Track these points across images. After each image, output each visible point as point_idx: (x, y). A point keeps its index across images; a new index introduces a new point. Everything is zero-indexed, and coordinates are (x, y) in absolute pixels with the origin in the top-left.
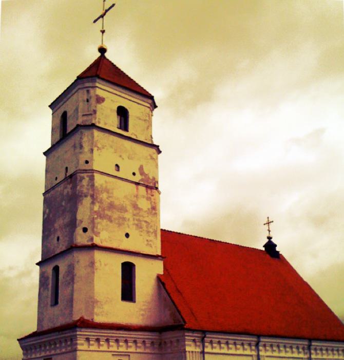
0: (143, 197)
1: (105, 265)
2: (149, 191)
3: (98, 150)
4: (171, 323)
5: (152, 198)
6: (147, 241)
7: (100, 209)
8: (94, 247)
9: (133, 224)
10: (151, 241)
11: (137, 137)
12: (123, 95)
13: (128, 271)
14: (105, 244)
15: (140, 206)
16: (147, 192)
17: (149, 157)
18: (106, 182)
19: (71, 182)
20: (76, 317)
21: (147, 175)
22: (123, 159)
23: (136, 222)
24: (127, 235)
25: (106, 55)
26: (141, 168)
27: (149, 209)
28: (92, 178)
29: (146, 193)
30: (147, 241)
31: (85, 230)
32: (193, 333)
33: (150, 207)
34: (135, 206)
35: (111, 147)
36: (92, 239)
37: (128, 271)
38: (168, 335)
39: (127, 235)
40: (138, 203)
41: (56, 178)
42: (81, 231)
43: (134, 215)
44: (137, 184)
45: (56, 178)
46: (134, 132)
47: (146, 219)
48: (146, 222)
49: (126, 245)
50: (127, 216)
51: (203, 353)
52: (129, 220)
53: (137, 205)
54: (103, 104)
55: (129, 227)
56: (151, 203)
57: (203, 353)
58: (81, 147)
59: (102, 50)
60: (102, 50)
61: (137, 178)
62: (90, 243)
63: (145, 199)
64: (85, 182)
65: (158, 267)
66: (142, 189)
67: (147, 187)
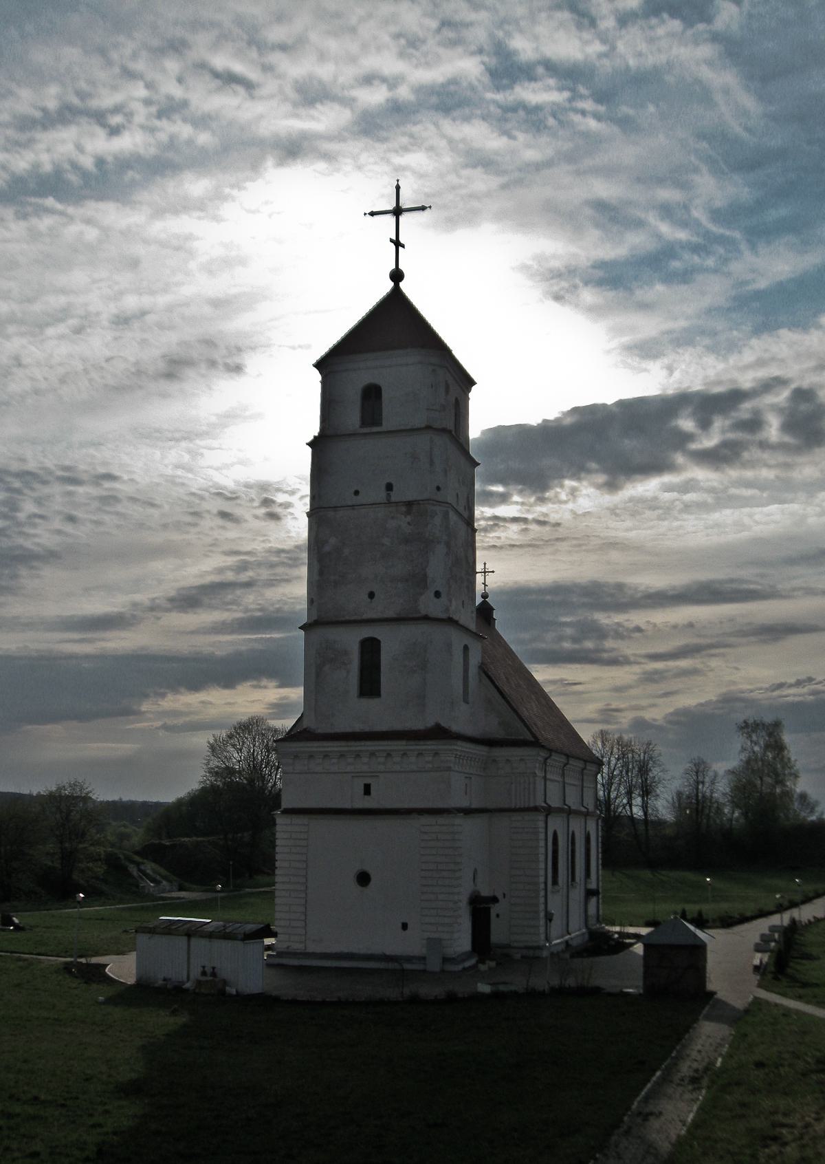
4: (500, 734)
8: (451, 621)
19: (408, 513)
20: (430, 722)
25: (402, 285)
28: (446, 515)
31: (437, 594)
36: (447, 610)
38: (501, 753)
41: (357, 493)
42: (432, 595)
45: (357, 493)
57: (545, 778)
58: (432, 463)
59: (397, 276)
60: (397, 276)
62: (444, 616)
64: (438, 520)
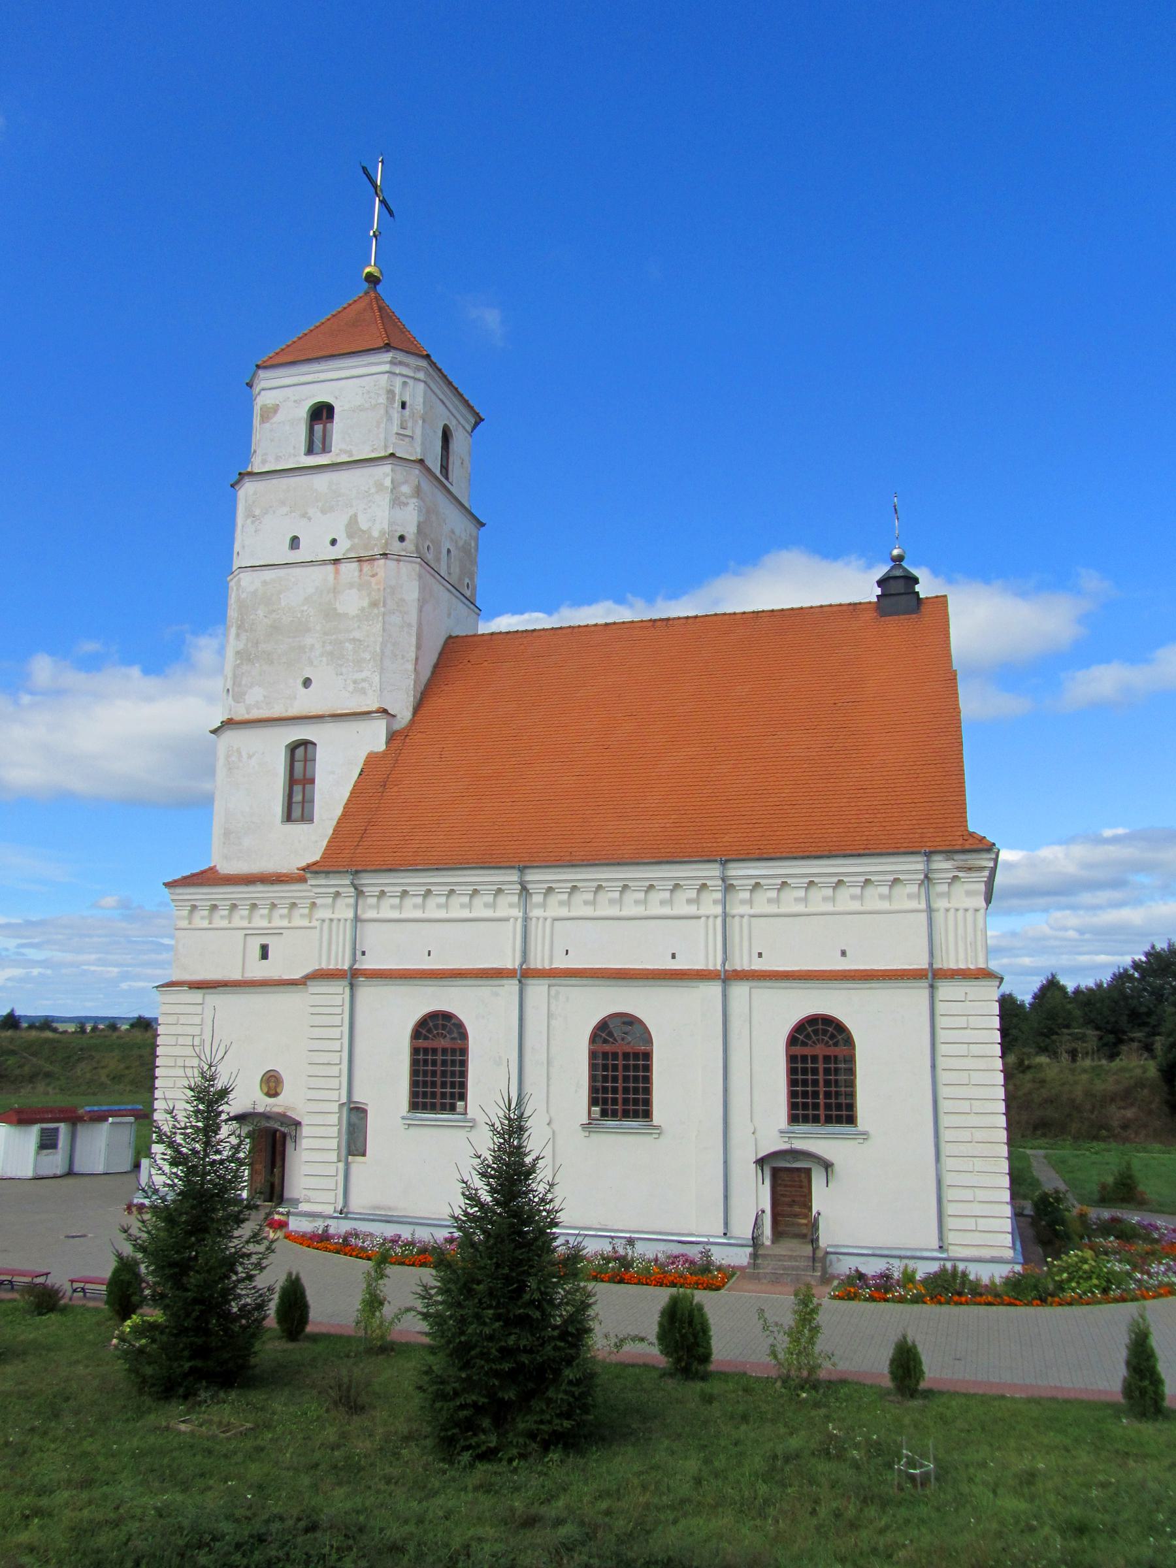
0: (351, 586)
1: (250, 757)
2: (366, 567)
3: (253, 522)
5: (373, 580)
6: (355, 682)
7: (250, 645)
9: (322, 655)
10: (363, 680)
11: (350, 454)
12: (322, 376)
13: (300, 754)
14: (256, 714)
15: (341, 609)
16: (361, 571)
17: (373, 490)
18: (265, 583)
21: (363, 532)
22: (310, 519)
23: (329, 648)
24: (307, 683)
26: (353, 521)
27: (363, 609)
29: (357, 574)
30: (355, 682)
32: (327, 877)
33: (365, 603)
34: (331, 614)
35: (283, 503)
37: (300, 754)
39: (307, 683)
40: (338, 605)
43: (325, 634)
44: (336, 561)
46: (344, 447)
47: (357, 634)
48: (354, 640)
49: (306, 702)
50: (309, 640)
51: (357, 919)
52: (312, 647)
53: (335, 609)
54: (275, 420)
55: (311, 663)
56: (369, 595)
61: (336, 553)
63: (354, 591)
65: (375, 737)
66: (349, 570)
67: (360, 560)
